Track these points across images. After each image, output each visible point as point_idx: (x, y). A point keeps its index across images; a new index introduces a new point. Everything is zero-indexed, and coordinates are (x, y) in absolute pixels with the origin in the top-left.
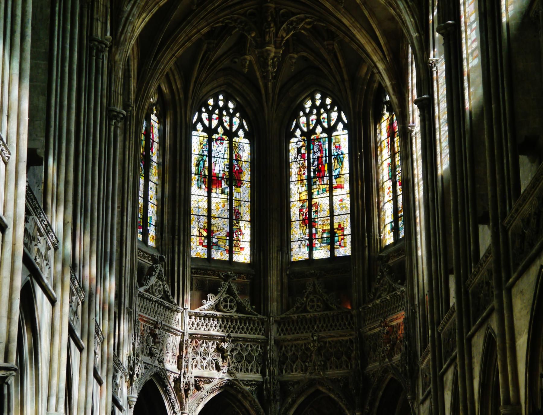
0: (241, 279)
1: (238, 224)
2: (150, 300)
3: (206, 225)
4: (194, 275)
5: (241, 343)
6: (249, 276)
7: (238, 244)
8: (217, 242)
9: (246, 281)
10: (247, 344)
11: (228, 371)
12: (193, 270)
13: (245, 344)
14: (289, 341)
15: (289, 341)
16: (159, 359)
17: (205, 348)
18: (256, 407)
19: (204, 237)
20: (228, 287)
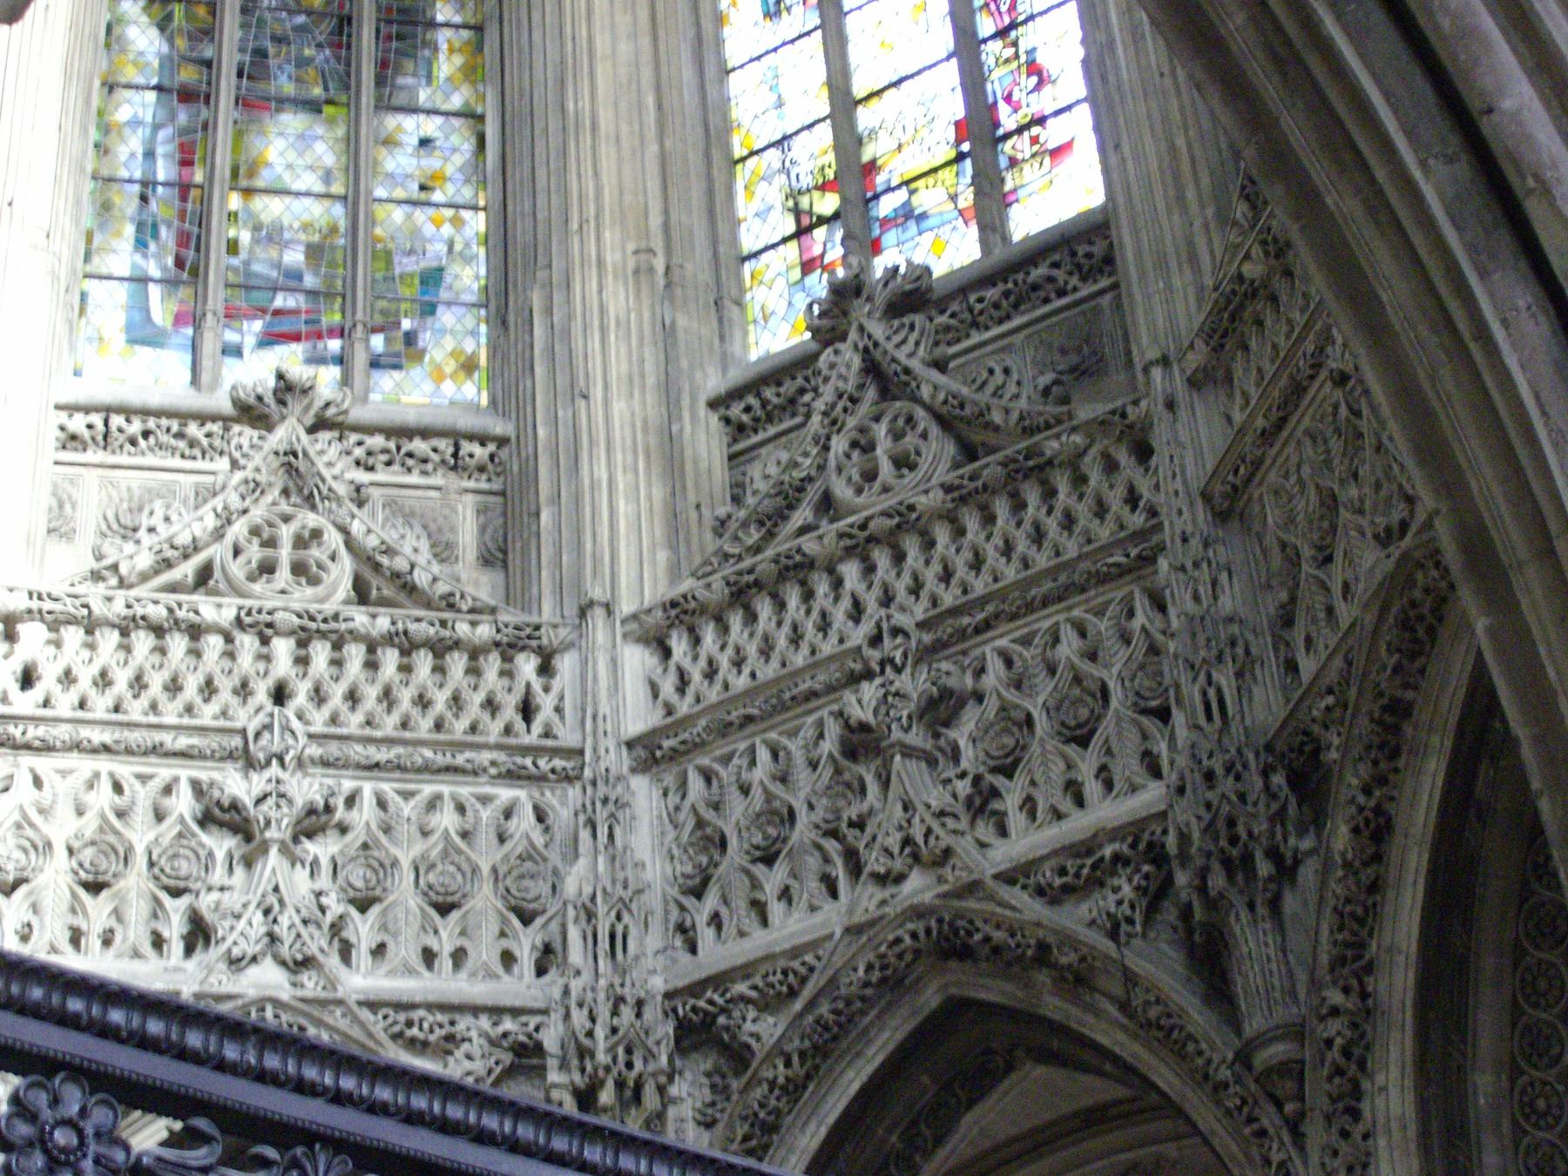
0: (1046, 301)
1: (1015, 44)
2: (195, 632)
3: (831, 157)
4: (755, 439)
5: (1002, 643)
6: (1081, 250)
7: (1034, 140)
8: (908, 202)
9: (1085, 291)
10: (1046, 624)
11: (916, 857)
12: (736, 411)
13: (1033, 634)
14: (1267, 436)
15: (1267, 436)
16: (285, 951)
17: (769, 797)
18: (1153, 1013)
19: (822, 221)
20: (858, 362)
